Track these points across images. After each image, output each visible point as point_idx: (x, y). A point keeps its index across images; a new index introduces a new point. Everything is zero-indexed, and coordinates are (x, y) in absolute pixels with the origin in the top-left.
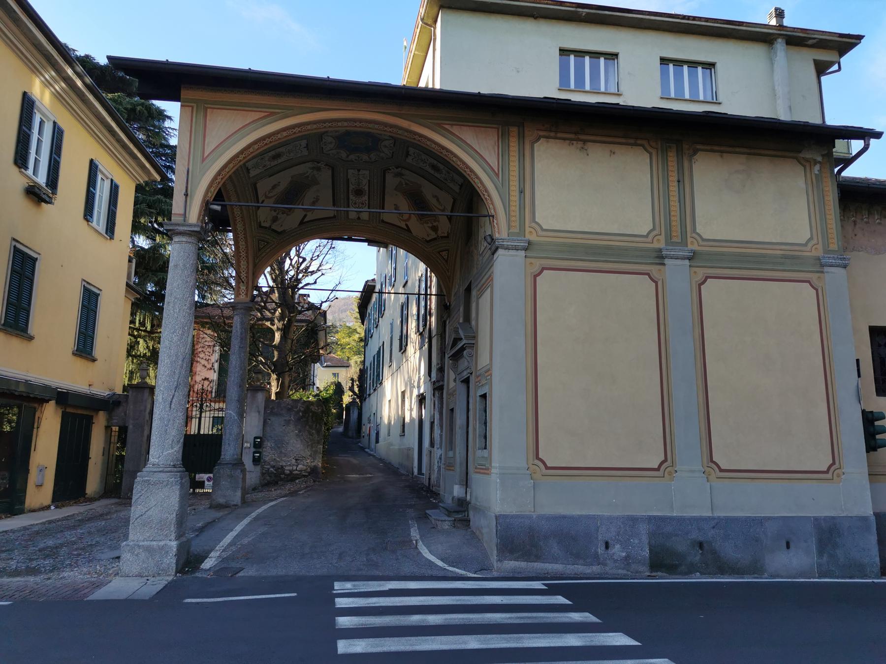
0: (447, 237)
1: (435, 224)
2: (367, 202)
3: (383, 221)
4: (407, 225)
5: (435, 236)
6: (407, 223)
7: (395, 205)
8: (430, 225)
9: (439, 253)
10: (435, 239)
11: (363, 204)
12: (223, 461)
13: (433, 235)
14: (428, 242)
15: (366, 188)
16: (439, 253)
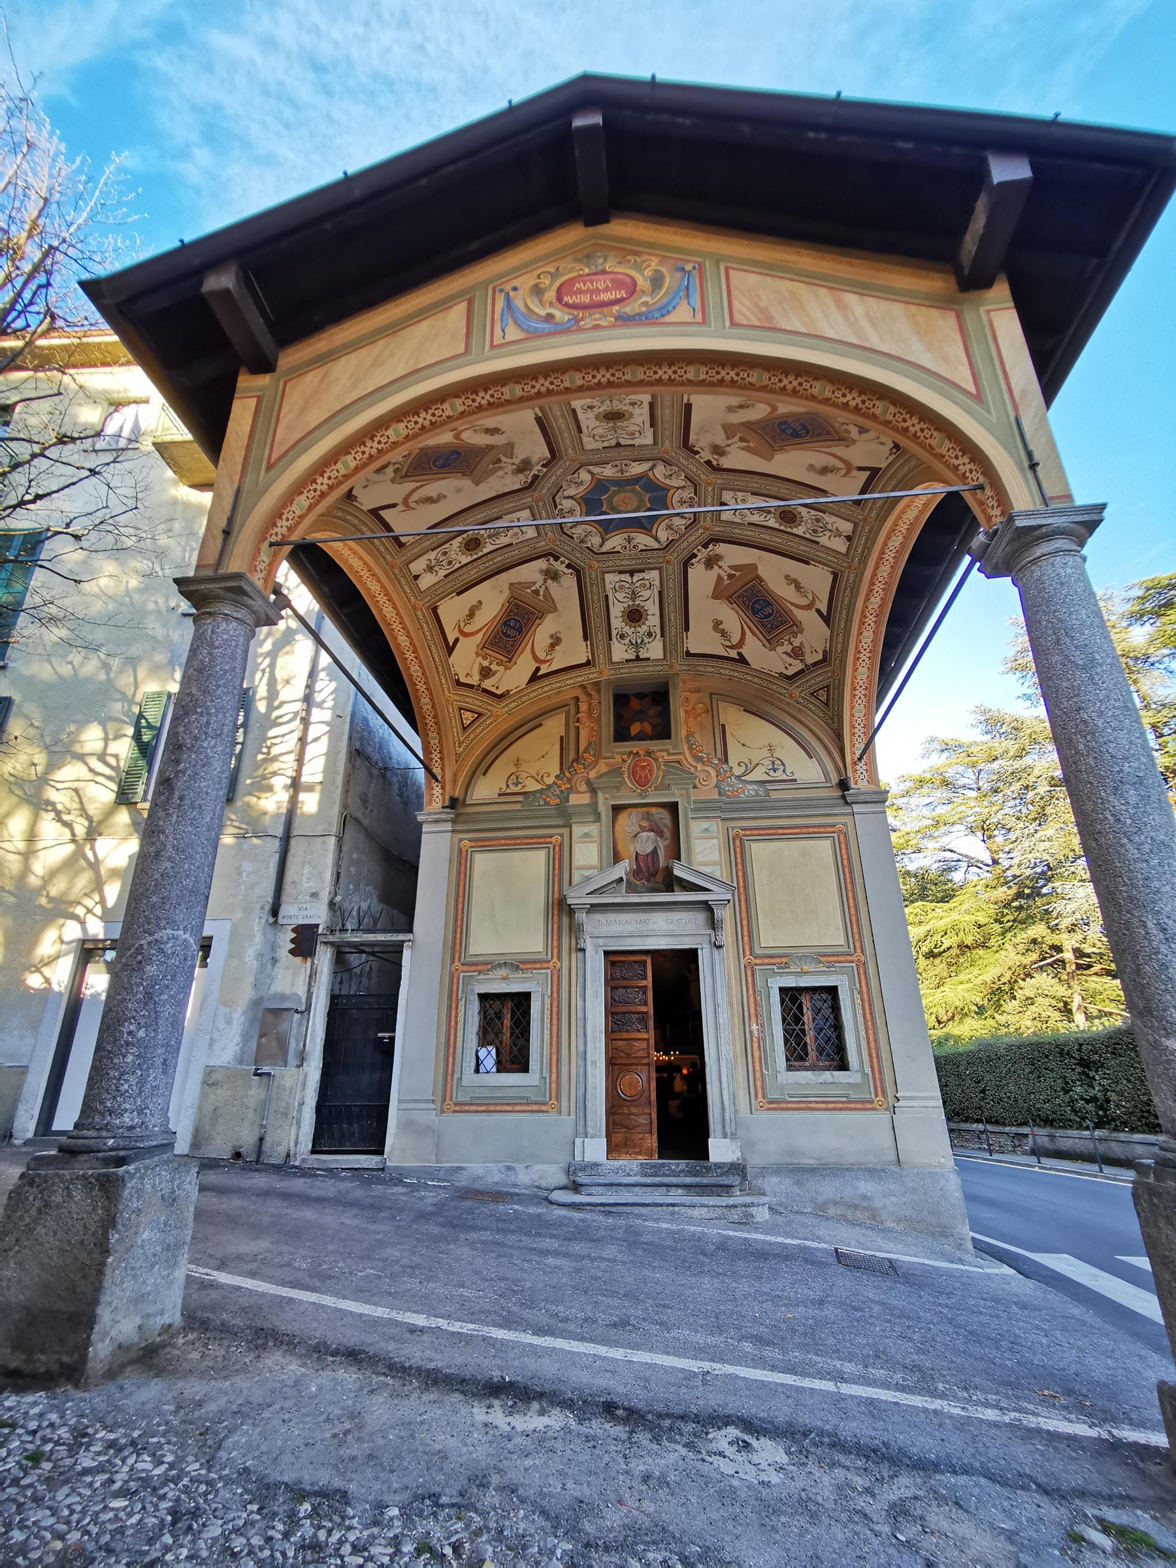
0: (500, 697)
1: (494, 667)
2: (458, 566)
3: (435, 610)
4: (457, 640)
5: (475, 683)
6: (461, 638)
7: (480, 602)
8: (486, 663)
9: (460, 709)
10: (471, 686)
11: (450, 563)
12: (142, 1138)
13: (474, 680)
14: (459, 683)
15: (489, 548)
16: (460, 709)
